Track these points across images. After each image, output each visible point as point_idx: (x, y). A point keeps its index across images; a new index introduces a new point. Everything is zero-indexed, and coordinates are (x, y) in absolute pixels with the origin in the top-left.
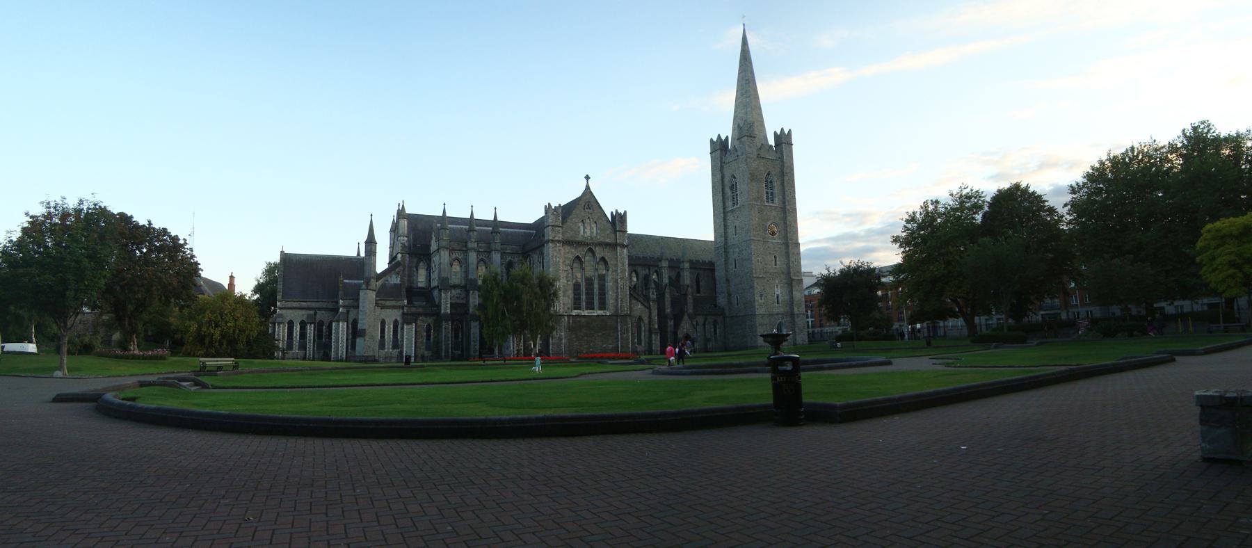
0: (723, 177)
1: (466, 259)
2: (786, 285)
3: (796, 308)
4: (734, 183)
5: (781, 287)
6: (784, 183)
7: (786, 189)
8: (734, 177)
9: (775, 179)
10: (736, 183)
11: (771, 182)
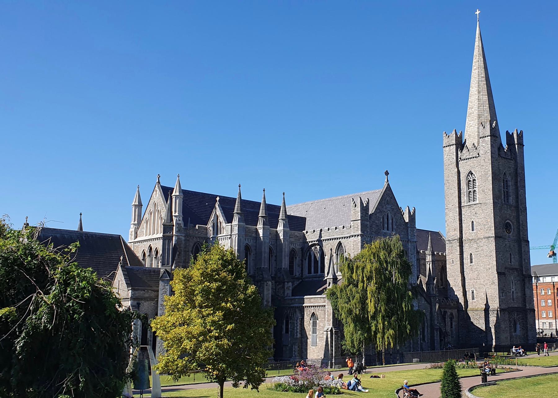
0: (459, 172)
1: (256, 247)
2: (519, 282)
3: (527, 305)
4: (471, 180)
5: (515, 284)
6: (517, 182)
7: (519, 189)
8: (472, 174)
9: (509, 178)
10: (474, 180)
11: (507, 181)
